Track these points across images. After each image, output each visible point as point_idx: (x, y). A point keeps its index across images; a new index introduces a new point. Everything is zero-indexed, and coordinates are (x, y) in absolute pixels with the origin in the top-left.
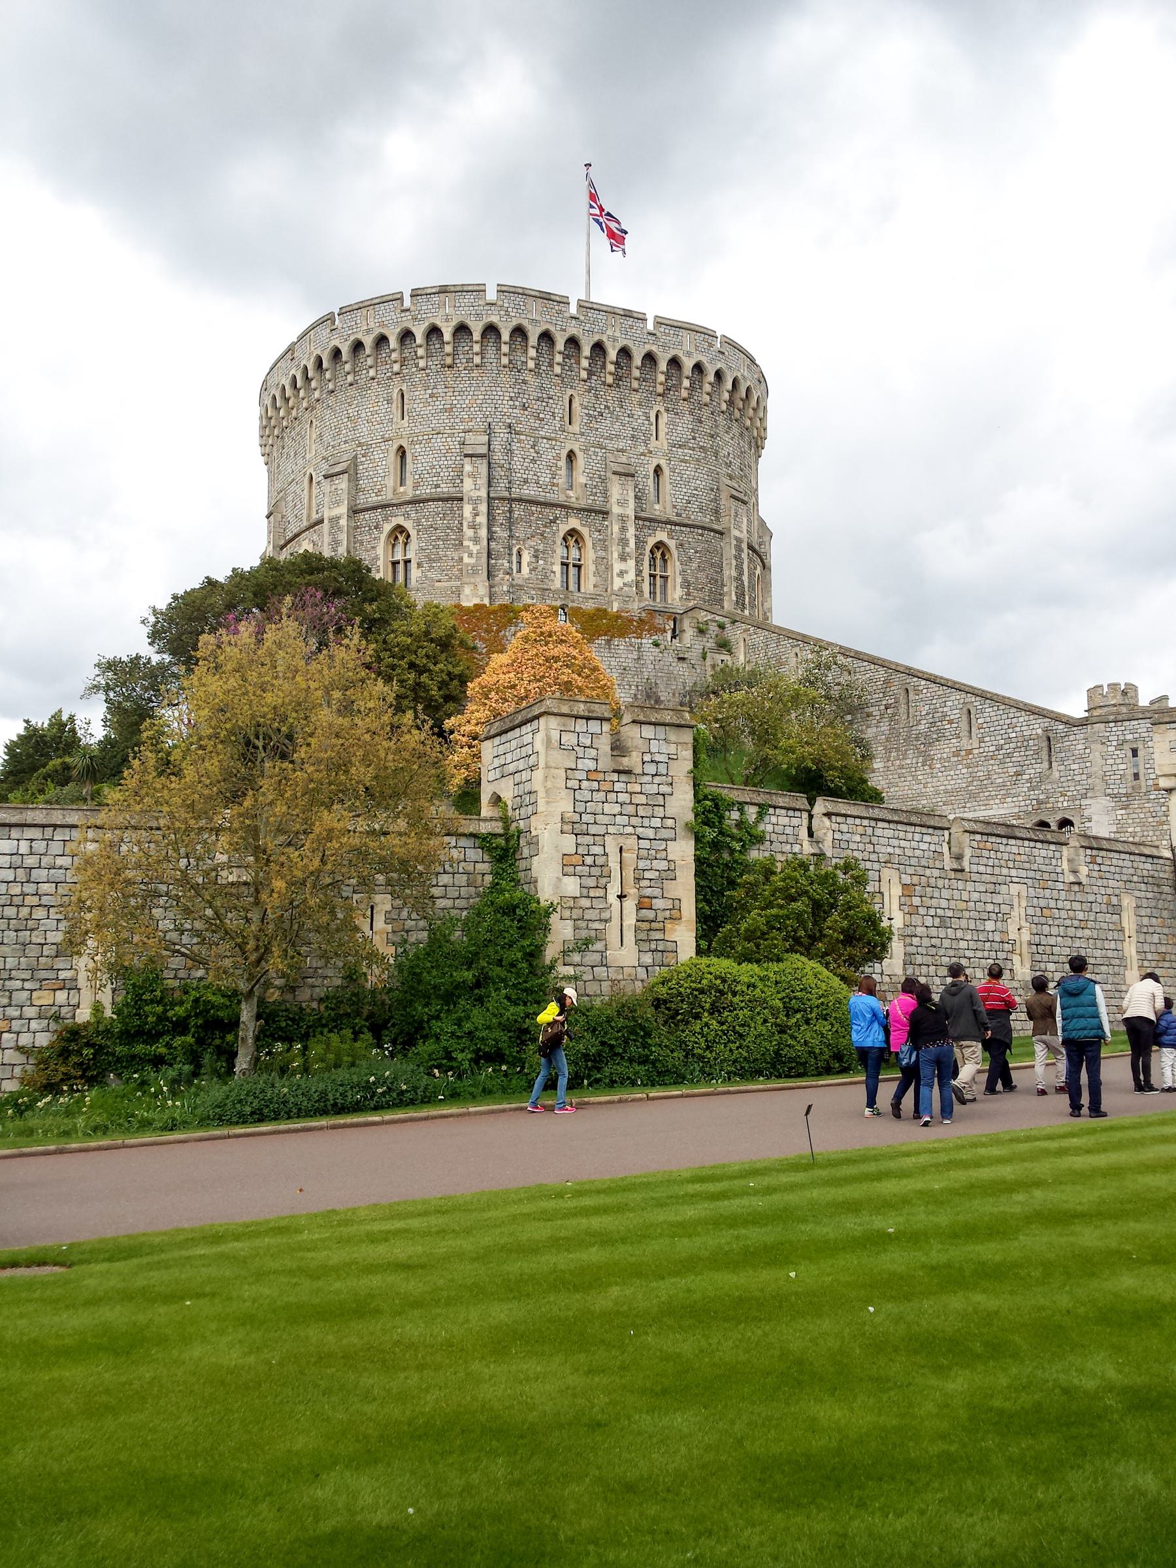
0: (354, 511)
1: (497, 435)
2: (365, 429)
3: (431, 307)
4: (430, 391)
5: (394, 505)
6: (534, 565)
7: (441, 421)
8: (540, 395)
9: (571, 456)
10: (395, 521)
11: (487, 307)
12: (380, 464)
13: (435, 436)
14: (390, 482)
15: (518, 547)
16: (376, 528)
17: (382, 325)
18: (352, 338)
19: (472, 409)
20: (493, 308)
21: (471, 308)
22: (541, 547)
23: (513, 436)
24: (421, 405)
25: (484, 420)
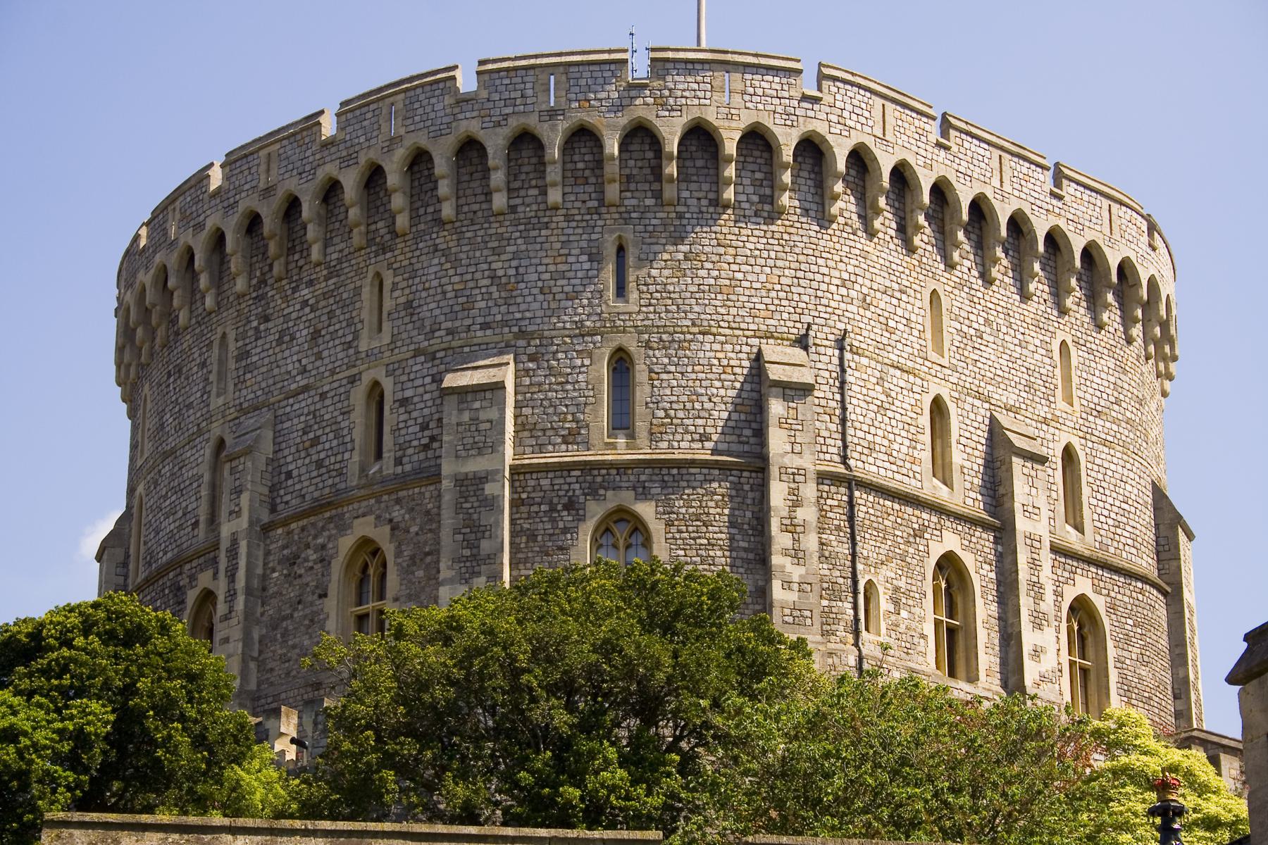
1: (822, 350)
2: (536, 306)
3: (695, 86)
6: (893, 617)
8: (888, 283)
9: (938, 409)
10: (612, 500)
13: (700, 337)
15: (867, 578)
16: (567, 507)
18: (514, 123)
19: (773, 294)
20: (816, 107)
21: (776, 101)
22: (902, 584)
25: (796, 317)
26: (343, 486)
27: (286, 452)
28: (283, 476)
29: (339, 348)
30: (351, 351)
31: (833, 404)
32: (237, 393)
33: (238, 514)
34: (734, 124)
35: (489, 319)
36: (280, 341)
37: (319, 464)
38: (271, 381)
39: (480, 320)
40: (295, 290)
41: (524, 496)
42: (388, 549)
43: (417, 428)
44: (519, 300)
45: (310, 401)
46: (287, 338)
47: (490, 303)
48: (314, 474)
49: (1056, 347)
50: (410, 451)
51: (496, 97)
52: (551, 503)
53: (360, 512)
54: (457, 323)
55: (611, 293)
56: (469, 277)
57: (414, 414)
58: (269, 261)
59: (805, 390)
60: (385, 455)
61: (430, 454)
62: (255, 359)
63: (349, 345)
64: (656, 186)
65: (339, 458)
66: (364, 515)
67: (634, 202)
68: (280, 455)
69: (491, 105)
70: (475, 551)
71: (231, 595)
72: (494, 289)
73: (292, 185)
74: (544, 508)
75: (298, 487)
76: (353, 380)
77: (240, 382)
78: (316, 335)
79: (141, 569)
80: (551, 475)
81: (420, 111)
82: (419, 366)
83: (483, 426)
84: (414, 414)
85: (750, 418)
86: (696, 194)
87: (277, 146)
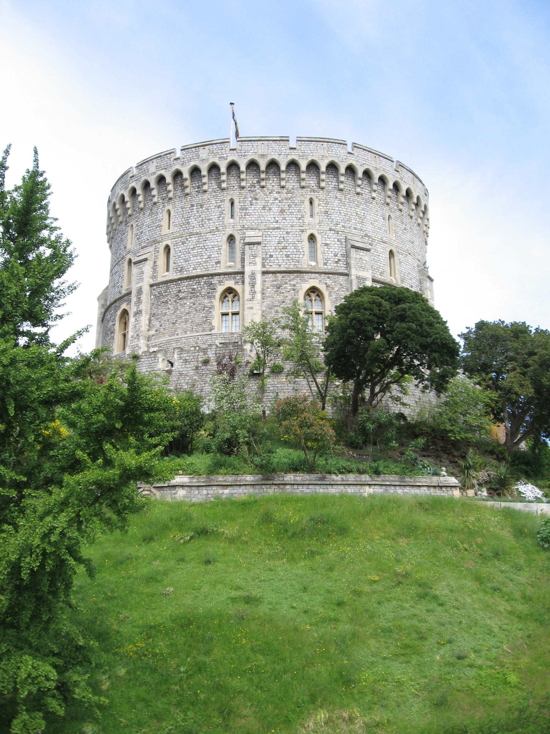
2: (369, 228)
17: (384, 170)
26: (300, 266)
28: (268, 256)
29: (294, 219)
30: (301, 221)
32: (241, 221)
35: (356, 227)
36: (264, 208)
37: (287, 256)
40: (270, 193)
42: (326, 293)
43: (333, 255)
45: (281, 233)
46: (267, 208)
50: (329, 262)
53: (312, 277)
54: (346, 224)
57: (331, 250)
63: (300, 219)
64: (397, 203)
65: (298, 256)
66: (314, 278)
72: (357, 217)
73: (276, 157)
75: (277, 261)
78: (282, 211)
82: (331, 234)
84: (331, 250)
87: (267, 142)
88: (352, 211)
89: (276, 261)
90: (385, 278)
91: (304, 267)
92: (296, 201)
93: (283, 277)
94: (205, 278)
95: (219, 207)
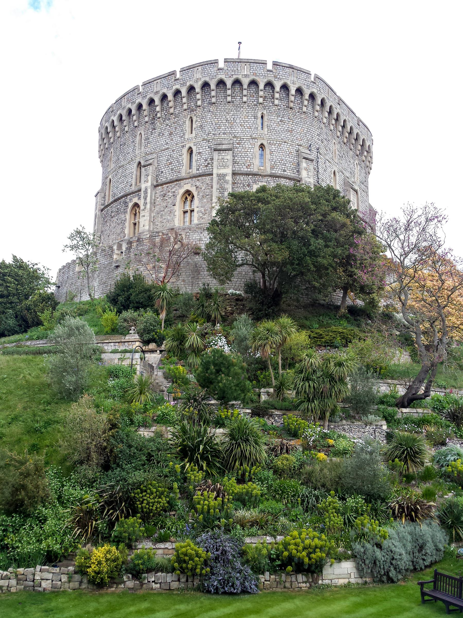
0: (234, 174)
1: (313, 152)
2: (238, 129)
4: (280, 119)
5: (260, 175)
7: (286, 136)
10: (261, 184)
11: (312, 84)
12: (249, 150)
13: (283, 143)
14: (257, 162)
16: (248, 185)
17: (255, 74)
18: (235, 77)
19: (302, 134)
20: (314, 85)
23: (319, 155)
24: (275, 124)
25: (307, 142)
26: (180, 176)
27: (161, 166)
28: (160, 173)
29: (178, 138)
30: (182, 138)
31: (315, 167)
33: (147, 182)
34: (295, 86)
35: (225, 132)
36: (159, 135)
37: (172, 169)
38: (156, 146)
39: (223, 132)
41: (236, 181)
42: (195, 194)
44: (234, 127)
45: (169, 152)
46: (161, 134)
47: (226, 127)
48: (171, 172)
49: (355, 164)
50: (201, 167)
51: (229, 69)
52: (243, 184)
55: (260, 128)
56: (220, 119)
57: (203, 157)
58: (155, 113)
59: (312, 161)
60: (193, 168)
61: (208, 168)
62: (151, 140)
64: (272, 100)
65: (179, 168)
67: (267, 104)
68: (159, 167)
69: (228, 71)
70: (223, 195)
71: (145, 204)
72: (227, 123)
73: (165, 91)
74: (241, 185)
75: (165, 175)
76: (183, 147)
77: (146, 146)
78: (171, 134)
79: (111, 198)
80: (243, 176)
81: (207, 71)
82: (204, 144)
83: (225, 161)
84: (203, 157)
85: (296, 167)
86: (283, 104)
87: (160, 80)
88: (222, 119)
89: (165, 175)
90: (252, 170)
91: (183, 174)
92: (180, 123)
93: (167, 187)
94: (123, 199)
95: (133, 142)
